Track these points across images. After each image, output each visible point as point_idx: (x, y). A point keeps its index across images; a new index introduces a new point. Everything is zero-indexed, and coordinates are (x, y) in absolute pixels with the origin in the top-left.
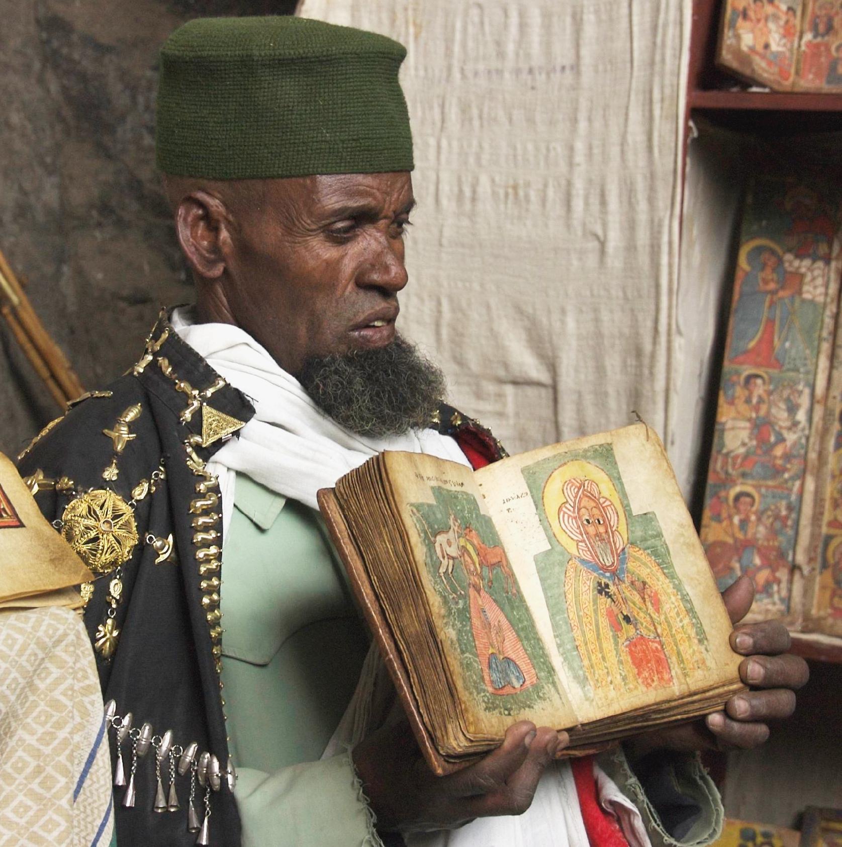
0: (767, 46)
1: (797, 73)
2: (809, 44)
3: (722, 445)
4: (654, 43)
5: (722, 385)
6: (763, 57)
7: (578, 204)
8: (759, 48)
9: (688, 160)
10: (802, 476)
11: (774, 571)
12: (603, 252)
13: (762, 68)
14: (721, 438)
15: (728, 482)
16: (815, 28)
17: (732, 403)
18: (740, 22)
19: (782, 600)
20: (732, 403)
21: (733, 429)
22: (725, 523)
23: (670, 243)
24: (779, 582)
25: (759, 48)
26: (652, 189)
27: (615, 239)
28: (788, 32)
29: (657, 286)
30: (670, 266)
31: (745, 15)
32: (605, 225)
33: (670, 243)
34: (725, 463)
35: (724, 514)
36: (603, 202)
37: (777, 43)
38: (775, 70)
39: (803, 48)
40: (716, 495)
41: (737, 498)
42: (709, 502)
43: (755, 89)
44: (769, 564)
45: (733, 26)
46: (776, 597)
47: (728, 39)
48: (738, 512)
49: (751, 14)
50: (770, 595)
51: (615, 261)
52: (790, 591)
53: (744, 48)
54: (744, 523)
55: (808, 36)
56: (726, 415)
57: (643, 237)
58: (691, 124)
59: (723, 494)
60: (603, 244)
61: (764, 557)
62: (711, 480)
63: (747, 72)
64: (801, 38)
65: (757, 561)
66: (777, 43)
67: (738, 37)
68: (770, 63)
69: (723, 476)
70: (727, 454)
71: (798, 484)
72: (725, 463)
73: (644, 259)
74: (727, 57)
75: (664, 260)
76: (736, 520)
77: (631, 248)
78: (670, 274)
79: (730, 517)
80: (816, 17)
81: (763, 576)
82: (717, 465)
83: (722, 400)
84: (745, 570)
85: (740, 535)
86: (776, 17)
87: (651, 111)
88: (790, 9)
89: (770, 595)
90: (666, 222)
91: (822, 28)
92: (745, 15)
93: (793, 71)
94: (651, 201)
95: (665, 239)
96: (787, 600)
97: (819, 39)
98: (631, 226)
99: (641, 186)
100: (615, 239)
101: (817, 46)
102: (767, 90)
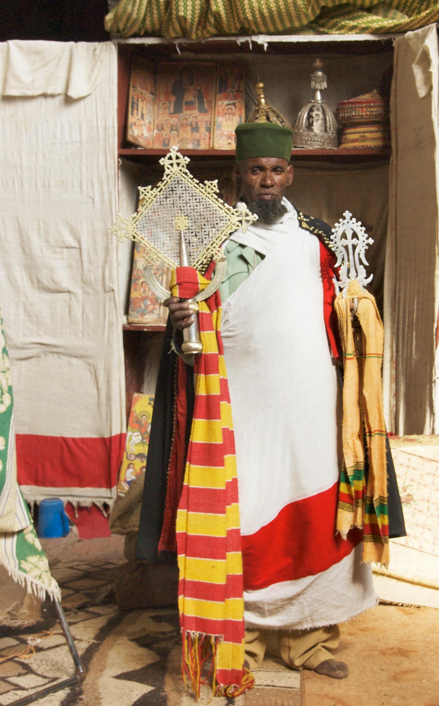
0: (142, 134)
1: (153, 143)
2: (156, 134)
3: (136, 266)
4: (106, 134)
5: (136, 247)
6: (142, 138)
7: (84, 187)
8: (140, 135)
9: (120, 172)
10: (162, 275)
11: (154, 305)
12: (93, 202)
13: (141, 142)
14: (136, 264)
15: (138, 278)
16: (158, 128)
17: (139, 252)
18: (133, 127)
19: (157, 315)
20: (139, 252)
21: (139, 261)
22: (138, 291)
23: (115, 198)
24: (156, 309)
25: (140, 135)
26: (108, 181)
27: (97, 198)
28: (149, 130)
29: (112, 213)
30: (116, 206)
31: (135, 125)
32: (94, 193)
33: (115, 198)
34: (137, 272)
35: (138, 288)
36: (93, 186)
37: (146, 134)
38: (146, 142)
39: (155, 135)
40: (135, 283)
41: (142, 283)
42: (133, 285)
43: (139, 148)
44: (153, 303)
45: (131, 128)
46: (155, 314)
47: (130, 132)
48: (142, 287)
49: (137, 124)
50: (153, 313)
51: (98, 205)
52: (160, 311)
53: (135, 135)
54: (144, 291)
55: (156, 131)
56: (137, 257)
57: (106, 197)
58: (120, 160)
59: (137, 282)
60: (93, 200)
61: (151, 301)
62: (133, 278)
63: (137, 143)
64: (153, 131)
65: (149, 303)
66: (146, 134)
67: (133, 131)
68: (144, 140)
69: (137, 276)
70: (138, 270)
71: (161, 278)
72: (137, 272)
73: (107, 205)
74: (130, 138)
75: (114, 204)
76: (142, 290)
77: (102, 201)
78: (116, 209)
79: (140, 289)
80: (158, 125)
81: (151, 307)
82: (135, 273)
83: (135, 252)
84: (145, 306)
85: (143, 295)
86: (145, 125)
87: (106, 156)
88: (149, 122)
89: (153, 313)
90: (113, 192)
91: (160, 128)
92: (135, 125)
93: (151, 142)
94: (108, 185)
95: (113, 197)
96: (159, 315)
97: (159, 132)
98: (102, 193)
99: (105, 180)
100: (97, 198)
101: (159, 134)
102: (142, 149)
